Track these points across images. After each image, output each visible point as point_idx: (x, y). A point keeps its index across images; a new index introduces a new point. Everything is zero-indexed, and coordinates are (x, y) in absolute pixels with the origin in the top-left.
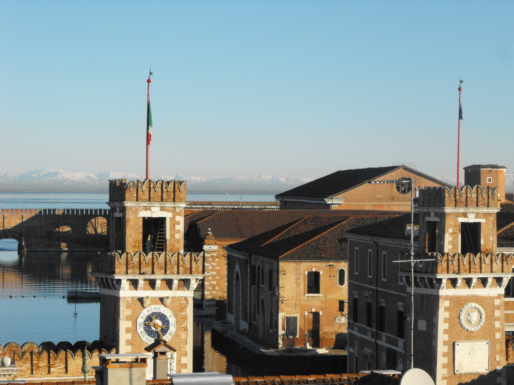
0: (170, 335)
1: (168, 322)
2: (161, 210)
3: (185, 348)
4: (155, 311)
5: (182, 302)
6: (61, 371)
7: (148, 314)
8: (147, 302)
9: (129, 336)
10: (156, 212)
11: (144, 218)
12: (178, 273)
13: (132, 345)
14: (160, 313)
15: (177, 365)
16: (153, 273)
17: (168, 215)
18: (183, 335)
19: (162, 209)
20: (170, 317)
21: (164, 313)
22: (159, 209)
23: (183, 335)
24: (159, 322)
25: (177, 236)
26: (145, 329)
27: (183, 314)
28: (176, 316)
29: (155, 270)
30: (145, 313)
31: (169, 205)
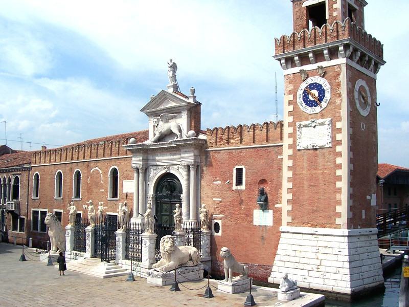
1: (324, 90)
3: (340, 113)
4: (312, 82)
5: (336, 70)
6: (237, 142)
9: (291, 108)
13: (293, 115)
14: (316, 83)
18: (338, 101)
20: (326, 86)
23: (338, 101)
25: (335, 14)
26: (304, 100)
27: (337, 81)
28: (331, 84)
30: (303, 86)
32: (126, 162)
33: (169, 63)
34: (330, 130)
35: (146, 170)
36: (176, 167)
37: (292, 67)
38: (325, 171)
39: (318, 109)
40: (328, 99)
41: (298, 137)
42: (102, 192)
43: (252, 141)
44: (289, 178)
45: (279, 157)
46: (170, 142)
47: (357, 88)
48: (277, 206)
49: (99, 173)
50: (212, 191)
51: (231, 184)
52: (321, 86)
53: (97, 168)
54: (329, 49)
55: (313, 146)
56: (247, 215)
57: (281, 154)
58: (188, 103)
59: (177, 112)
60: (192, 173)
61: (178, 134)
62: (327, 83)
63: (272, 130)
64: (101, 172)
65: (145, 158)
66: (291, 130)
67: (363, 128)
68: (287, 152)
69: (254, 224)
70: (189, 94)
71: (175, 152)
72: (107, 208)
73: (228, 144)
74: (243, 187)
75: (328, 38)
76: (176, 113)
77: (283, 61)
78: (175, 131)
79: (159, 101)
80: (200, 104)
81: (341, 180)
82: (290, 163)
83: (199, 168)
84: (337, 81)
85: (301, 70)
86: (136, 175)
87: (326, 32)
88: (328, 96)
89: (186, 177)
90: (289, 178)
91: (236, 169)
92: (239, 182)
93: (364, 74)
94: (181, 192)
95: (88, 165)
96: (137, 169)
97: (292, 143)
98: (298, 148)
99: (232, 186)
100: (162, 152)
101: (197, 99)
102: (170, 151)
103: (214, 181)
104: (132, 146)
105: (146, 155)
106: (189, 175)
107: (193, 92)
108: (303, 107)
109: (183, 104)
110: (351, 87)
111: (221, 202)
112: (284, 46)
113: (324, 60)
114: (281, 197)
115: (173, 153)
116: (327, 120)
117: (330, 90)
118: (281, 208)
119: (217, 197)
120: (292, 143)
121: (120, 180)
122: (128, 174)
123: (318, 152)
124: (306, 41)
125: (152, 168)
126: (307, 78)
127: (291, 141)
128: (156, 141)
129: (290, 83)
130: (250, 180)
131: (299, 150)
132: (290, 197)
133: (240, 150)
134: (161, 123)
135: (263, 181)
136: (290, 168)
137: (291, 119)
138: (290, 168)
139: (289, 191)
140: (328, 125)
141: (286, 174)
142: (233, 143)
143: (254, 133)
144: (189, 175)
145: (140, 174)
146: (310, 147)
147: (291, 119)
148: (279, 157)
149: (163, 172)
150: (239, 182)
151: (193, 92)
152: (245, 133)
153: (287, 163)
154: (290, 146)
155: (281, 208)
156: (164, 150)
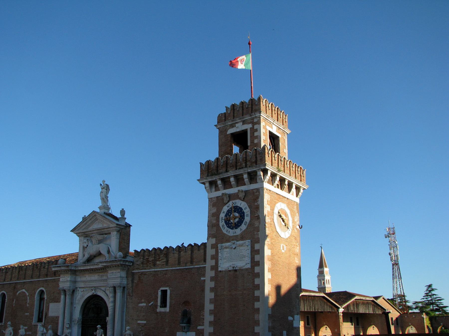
0: (245, 224)
1: (244, 213)
2: (243, 124)
3: (258, 235)
6: (163, 263)
7: (227, 209)
8: (226, 200)
10: (240, 127)
11: (232, 134)
12: (246, 167)
14: (237, 206)
15: (251, 252)
16: (227, 171)
17: (248, 127)
19: (244, 122)
20: (245, 208)
21: (241, 206)
22: (241, 123)
23: (256, 224)
24: (237, 215)
26: (225, 222)
27: (256, 204)
28: (250, 207)
29: (228, 169)
30: (225, 209)
31: (247, 118)
33: (101, 185)
34: (250, 250)
35: (74, 291)
36: (103, 288)
37: (216, 191)
38: (244, 292)
39: (238, 231)
40: (248, 222)
41: (219, 258)
42: (27, 316)
43: (177, 262)
44: (211, 300)
45: (202, 279)
46: (98, 263)
47: (276, 211)
48: (199, 328)
52: (241, 209)
53: (24, 290)
54: (249, 174)
55: (233, 267)
57: (204, 275)
58: (117, 224)
59: (107, 232)
60: (119, 294)
61: (107, 255)
62: (246, 206)
63: (196, 251)
64: (27, 294)
65: (73, 279)
66: (213, 252)
67: (283, 249)
68: (210, 274)
70: (118, 215)
71: (103, 274)
73: (154, 266)
74: (167, 309)
75: (248, 163)
76: (106, 234)
77: (207, 184)
78: (104, 252)
79: (90, 222)
80: (130, 226)
81: (259, 301)
82: (212, 284)
83: (126, 289)
84: (256, 204)
85: (223, 194)
86: (62, 297)
87: (246, 158)
88: (247, 219)
89: (112, 299)
90: (211, 300)
91: (162, 290)
92: (164, 304)
93: (285, 197)
94: (107, 315)
95: (15, 287)
96: (65, 291)
97: (214, 264)
98: (220, 269)
99: (157, 308)
100: (91, 273)
101: (127, 221)
102: (98, 273)
104: (60, 267)
105: (74, 277)
106: (115, 297)
107: (123, 212)
108: (226, 230)
109: (112, 225)
110: (269, 210)
111: (145, 324)
112: (208, 170)
113: (245, 184)
114: (204, 319)
115: (101, 274)
116: (248, 242)
117: (249, 213)
118: (203, 330)
119: (142, 320)
120: (214, 264)
121: (46, 303)
123: (238, 273)
124: (228, 166)
125: (81, 290)
126: (229, 201)
127: (213, 263)
128: (84, 263)
129: (213, 206)
131: (220, 271)
132: (212, 318)
134: (90, 244)
135: (186, 303)
136: (212, 290)
137: (213, 241)
138: (212, 290)
139: (211, 312)
140: (247, 246)
141: (209, 295)
142: (159, 264)
143: (179, 255)
144: (115, 297)
145: (67, 296)
146: (231, 269)
147: (213, 241)
148: (202, 279)
149: (90, 294)
150: (164, 304)
151: (123, 212)
152: (171, 255)
153: (209, 284)
154: (212, 268)
155: (203, 330)
156: (91, 272)
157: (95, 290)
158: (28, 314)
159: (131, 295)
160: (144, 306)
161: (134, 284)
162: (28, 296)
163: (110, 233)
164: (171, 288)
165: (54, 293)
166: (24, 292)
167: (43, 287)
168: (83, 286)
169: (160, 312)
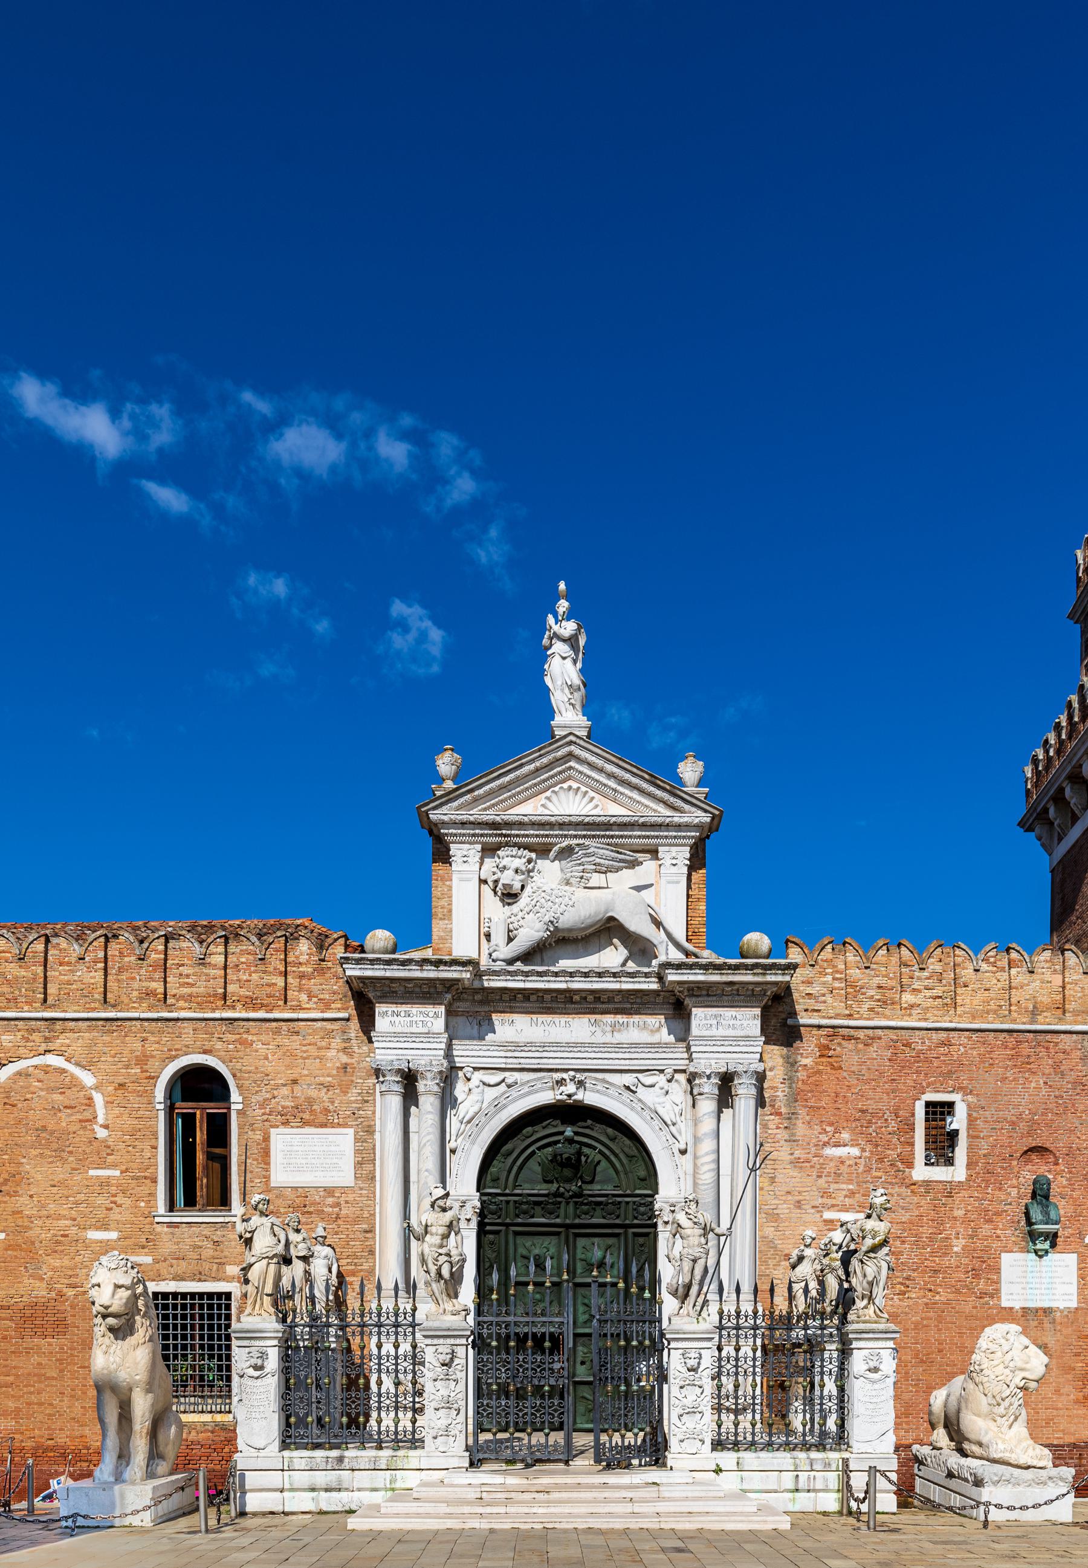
32: (295, 1043)
42: (105, 1183)
49: (75, 1084)
50: (822, 1182)
51: (910, 1165)
53: (52, 1060)
56: (976, 1274)
64: (87, 1079)
69: (1005, 1303)
71: (621, 1018)
72: (148, 1260)
74: (958, 1172)
102: (593, 1012)
103: (825, 1144)
115: (609, 1019)
122: (310, 1101)
125: (477, 1077)
130: (984, 1147)
133: (943, 1035)
135: (1039, 1150)
142: (912, 1006)
149: (546, 1097)
157: (581, 1084)
158: (117, 1173)
159: (783, 1110)
160: (849, 1158)
161: (801, 1075)
162: (96, 1088)
163: (654, 853)
164: (970, 1098)
165: (295, 1082)
166: (64, 1071)
167: (205, 1052)
168: (500, 1063)
169: (927, 1184)
